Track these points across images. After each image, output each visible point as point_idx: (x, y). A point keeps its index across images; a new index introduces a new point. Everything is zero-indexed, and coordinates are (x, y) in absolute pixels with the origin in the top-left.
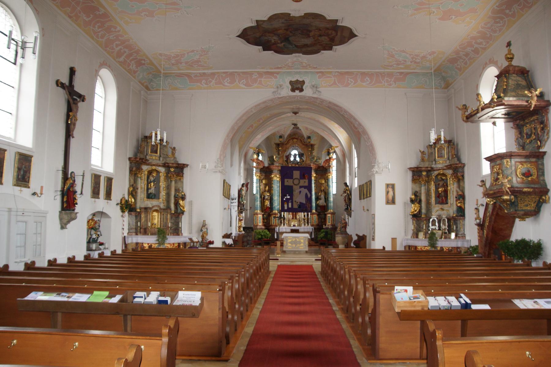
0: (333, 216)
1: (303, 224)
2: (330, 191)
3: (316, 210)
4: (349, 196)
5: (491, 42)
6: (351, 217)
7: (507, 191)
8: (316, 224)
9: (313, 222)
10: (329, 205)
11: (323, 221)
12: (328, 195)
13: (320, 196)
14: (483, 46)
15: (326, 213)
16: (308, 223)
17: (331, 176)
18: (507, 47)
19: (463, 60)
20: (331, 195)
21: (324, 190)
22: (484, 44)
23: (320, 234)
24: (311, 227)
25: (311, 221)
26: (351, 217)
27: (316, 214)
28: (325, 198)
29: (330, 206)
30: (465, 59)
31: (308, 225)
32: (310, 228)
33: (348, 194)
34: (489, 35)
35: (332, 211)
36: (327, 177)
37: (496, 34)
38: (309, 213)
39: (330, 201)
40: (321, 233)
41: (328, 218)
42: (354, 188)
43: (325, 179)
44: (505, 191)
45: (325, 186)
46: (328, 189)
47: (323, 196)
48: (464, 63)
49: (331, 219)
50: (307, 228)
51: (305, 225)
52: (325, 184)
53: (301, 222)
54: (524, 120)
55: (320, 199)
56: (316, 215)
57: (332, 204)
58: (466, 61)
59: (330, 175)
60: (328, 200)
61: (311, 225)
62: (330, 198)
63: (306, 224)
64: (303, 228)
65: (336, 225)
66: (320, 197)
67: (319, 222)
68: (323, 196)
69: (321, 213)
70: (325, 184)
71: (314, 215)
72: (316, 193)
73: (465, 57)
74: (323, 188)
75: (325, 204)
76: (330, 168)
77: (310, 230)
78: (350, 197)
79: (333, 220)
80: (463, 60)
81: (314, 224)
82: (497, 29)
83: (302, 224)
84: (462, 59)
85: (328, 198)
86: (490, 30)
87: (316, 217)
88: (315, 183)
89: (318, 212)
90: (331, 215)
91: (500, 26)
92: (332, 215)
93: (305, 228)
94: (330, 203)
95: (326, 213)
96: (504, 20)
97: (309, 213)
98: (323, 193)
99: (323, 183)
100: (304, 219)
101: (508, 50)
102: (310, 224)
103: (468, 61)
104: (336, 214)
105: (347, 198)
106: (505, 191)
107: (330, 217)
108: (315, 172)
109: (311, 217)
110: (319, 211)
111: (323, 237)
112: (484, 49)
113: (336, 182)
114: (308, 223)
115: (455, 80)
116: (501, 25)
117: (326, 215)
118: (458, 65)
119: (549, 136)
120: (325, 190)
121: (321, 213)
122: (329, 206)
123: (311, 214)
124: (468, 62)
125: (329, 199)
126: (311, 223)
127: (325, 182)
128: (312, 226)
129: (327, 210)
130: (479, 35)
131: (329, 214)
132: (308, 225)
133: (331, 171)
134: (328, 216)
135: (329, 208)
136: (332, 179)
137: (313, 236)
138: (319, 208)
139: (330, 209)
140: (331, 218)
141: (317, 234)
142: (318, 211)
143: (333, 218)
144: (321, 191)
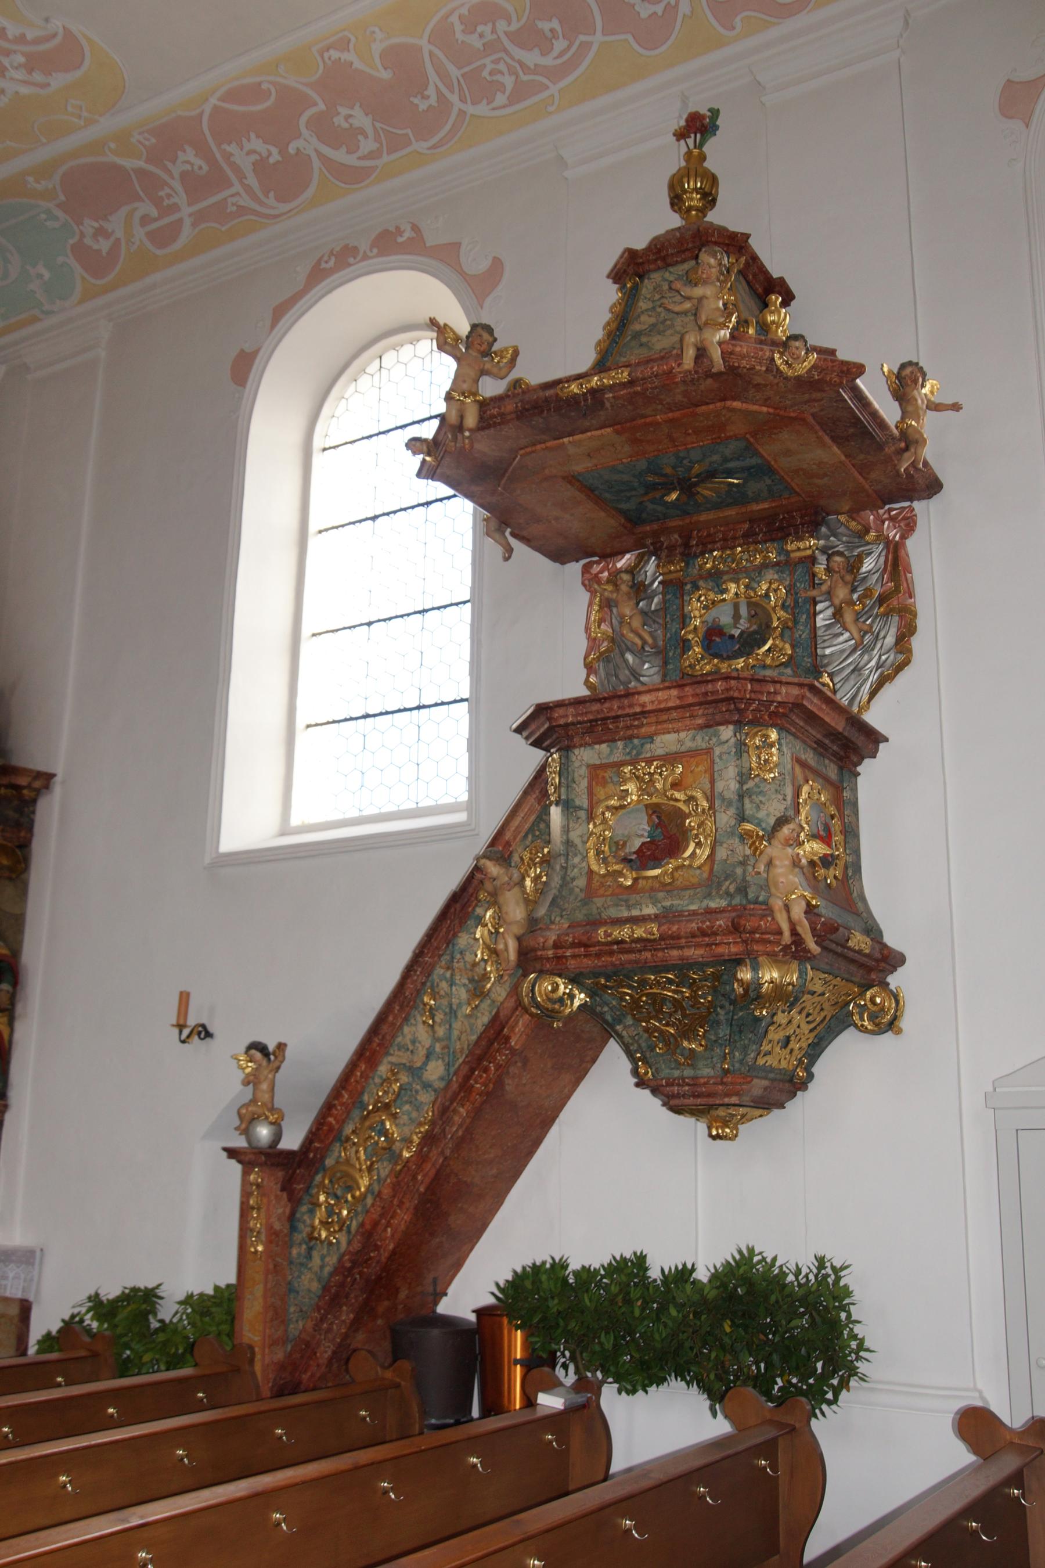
5: (422, 146)
7: (794, 932)
14: (351, 160)
18: (681, 135)
19: (154, 213)
22: (367, 145)
30: (175, 208)
34: (433, 100)
37: (482, 109)
44: (785, 927)
48: (150, 235)
54: (688, 556)
58: (180, 221)
73: (181, 198)
80: (154, 213)
82: (509, 81)
84: (157, 202)
86: (454, 72)
91: (537, 69)
96: (582, 38)
101: (689, 154)
103: (188, 222)
106: (785, 927)
112: (353, 176)
115: (35, 320)
116: (548, 61)
118: (101, 232)
119: (909, 651)
124: (186, 233)
130: (385, 75)
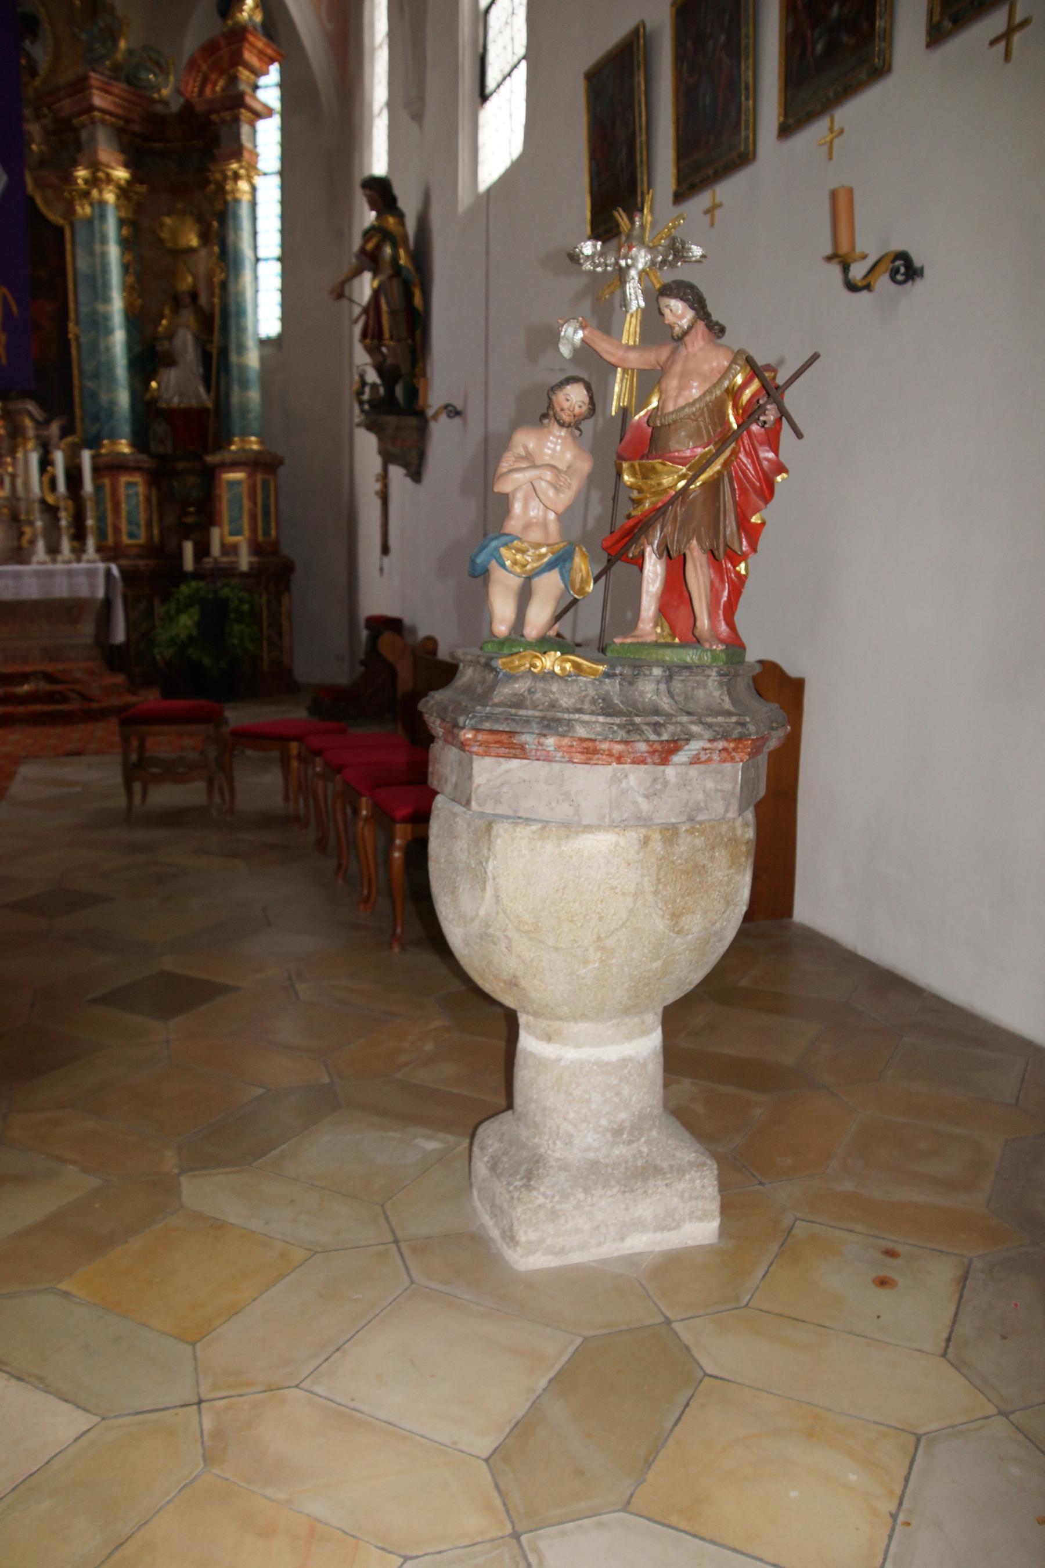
0: (265, 484)
1: (40, 545)
2: (240, 294)
3: (139, 441)
4: (409, 296)
6: (416, 474)
8: (142, 540)
9: (117, 530)
10: (235, 399)
11: (190, 520)
12: (225, 329)
13: (170, 335)
15: (210, 459)
16: (79, 536)
17: (243, 185)
20: (251, 344)
21: (194, 296)
23: (170, 618)
24: (101, 566)
25: (101, 519)
26: (416, 474)
27: (137, 469)
28: (206, 358)
29: (244, 411)
31: (79, 551)
32: (91, 573)
33: (397, 270)
35: (254, 444)
36: (221, 189)
38: (86, 456)
39: (243, 368)
40: (180, 611)
41: (225, 497)
42: (464, 200)
43: (200, 219)
45: (202, 270)
46: (224, 285)
47: (189, 337)
49: (246, 504)
50: (70, 573)
51: (53, 550)
52: (203, 253)
53: (28, 530)
55: (169, 361)
56: (137, 478)
57: (254, 395)
59: (236, 177)
60: (225, 366)
61: (99, 549)
62: (241, 348)
63: (66, 545)
64: (38, 574)
65: (286, 550)
66: (163, 346)
67: (162, 532)
68: (185, 342)
69: (180, 466)
70: (203, 253)
71: (124, 479)
72: (135, 320)
74: (190, 279)
75: (207, 400)
76: (236, 120)
77: (93, 587)
78: (418, 300)
79: (266, 513)
81: (126, 540)
83: (32, 542)
85: (224, 352)
87: (141, 489)
88: (125, 244)
89: (152, 456)
90: (251, 476)
92: (259, 477)
93: (50, 574)
94: (244, 385)
95: (210, 459)
97: (86, 456)
98: (188, 316)
99: (192, 250)
100: (51, 511)
102: (91, 543)
104: (282, 471)
105: (392, 313)
107: (244, 489)
108: (123, 150)
109: (98, 488)
110: (161, 450)
111: (191, 638)
113: (277, 252)
114: (79, 536)
117: (210, 475)
120: (203, 300)
121: (180, 466)
122: (235, 414)
123: (96, 470)
125: (234, 358)
126: (101, 534)
127: (205, 237)
128: (107, 553)
129: (222, 441)
131: (234, 466)
132: (79, 551)
133: (246, 142)
134: (231, 484)
135: (237, 427)
136: (253, 204)
137: (120, 636)
138: (161, 428)
139: (244, 434)
140: (253, 499)
141: (150, 612)
142: (153, 447)
143: (266, 497)
144: (177, 302)
